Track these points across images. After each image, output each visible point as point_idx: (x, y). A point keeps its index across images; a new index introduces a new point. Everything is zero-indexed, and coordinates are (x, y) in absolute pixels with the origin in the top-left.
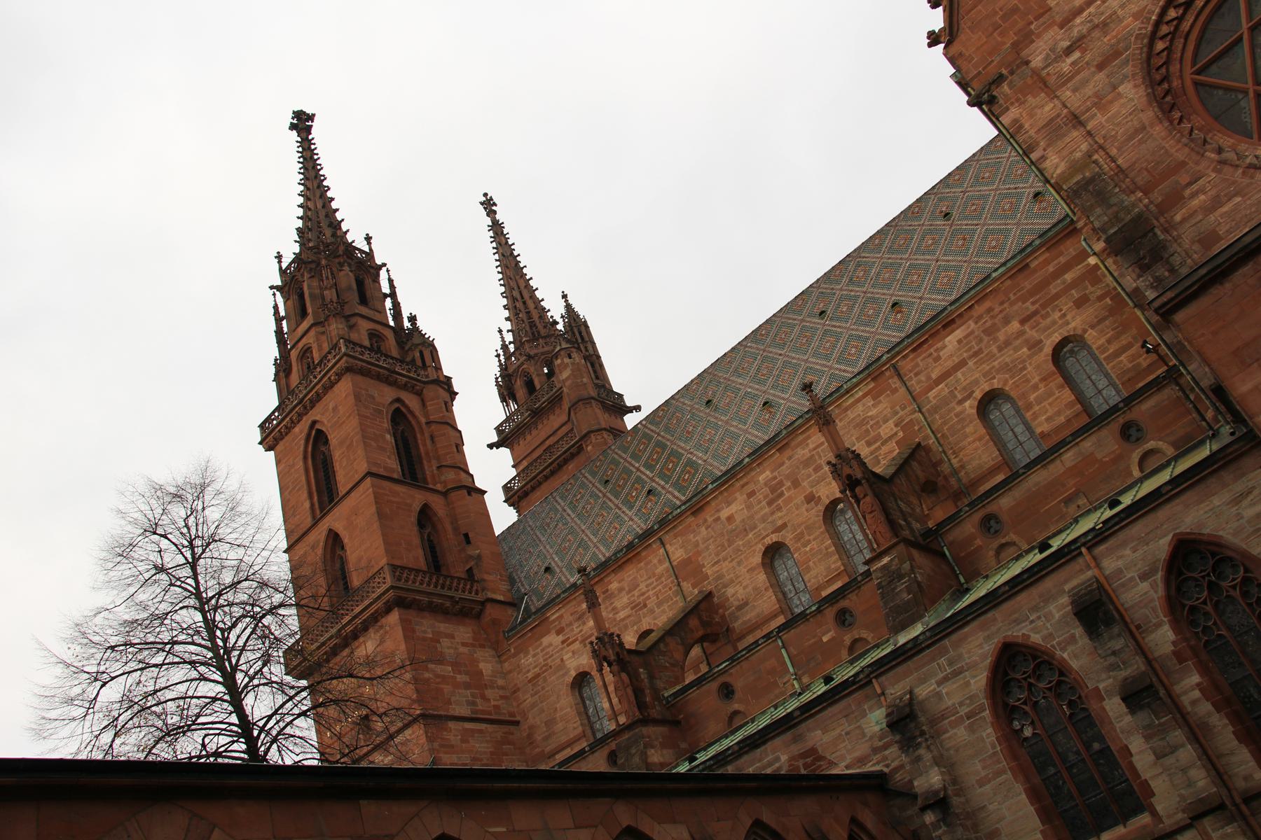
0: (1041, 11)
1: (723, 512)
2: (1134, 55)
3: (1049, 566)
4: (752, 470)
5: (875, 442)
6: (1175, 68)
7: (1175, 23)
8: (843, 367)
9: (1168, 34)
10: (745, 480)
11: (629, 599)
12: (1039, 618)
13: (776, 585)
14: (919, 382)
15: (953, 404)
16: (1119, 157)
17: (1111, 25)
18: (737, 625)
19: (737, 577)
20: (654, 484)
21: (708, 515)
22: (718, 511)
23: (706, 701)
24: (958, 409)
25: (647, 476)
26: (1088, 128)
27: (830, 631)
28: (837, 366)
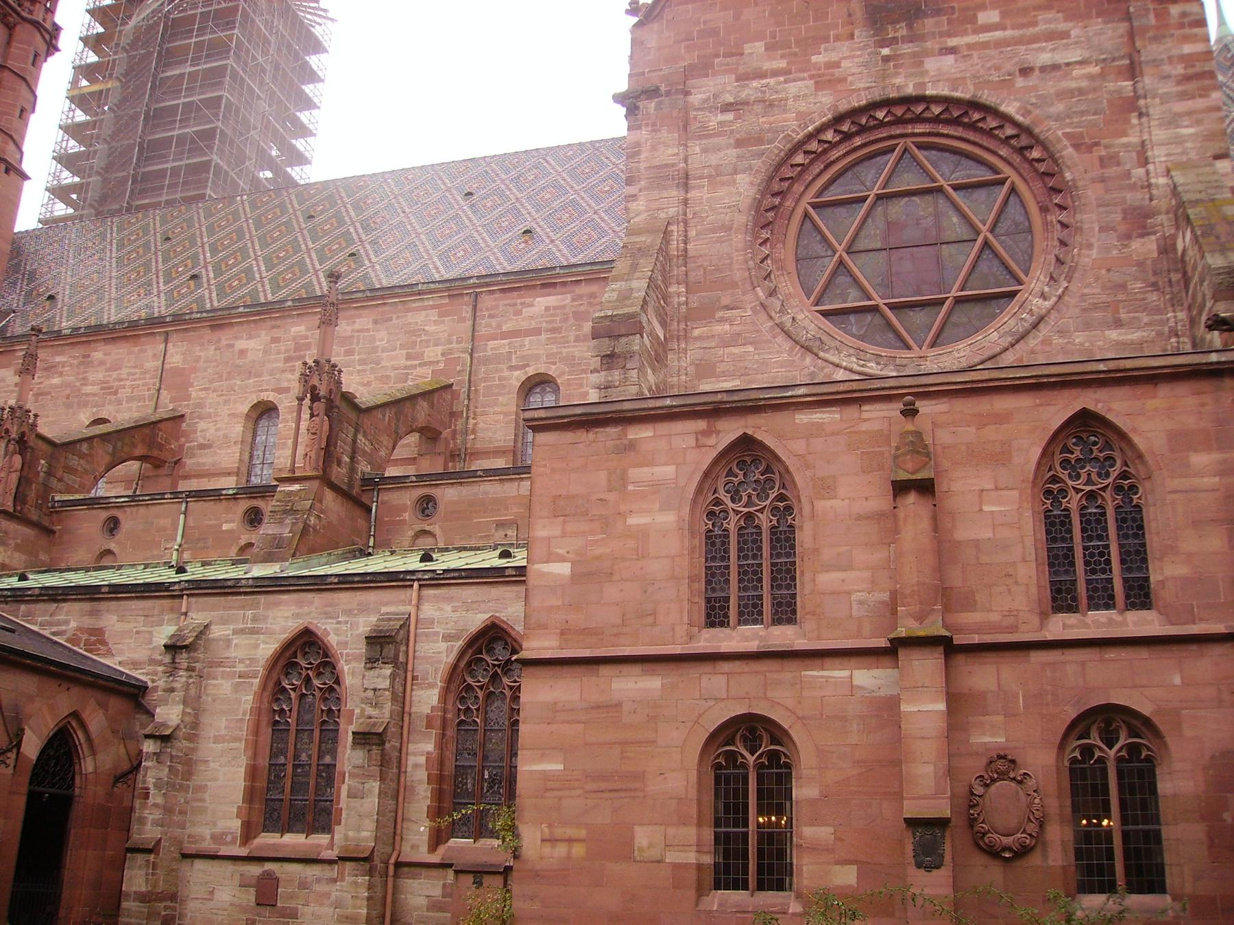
0: (734, 50)
1: (239, 342)
2: (772, 152)
3: (380, 582)
4: (290, 316)
5: (415, 359)
6: (798, 188)
7: (826, 146)
8: (439, 264)
9: (815, 152)
10: (278, 322)
11: (104, 376)
12: (346, 622)
13: (251, 444)
14: (489, 325)
16: (694, 241)
18: (189, 463)
19: (217, 415)
20: (204, 272)
21: (225, 337)
22: (236, 338)
23: (89, 524)
24: (506, 373)
25: (205, 258)
27: (232, 521)
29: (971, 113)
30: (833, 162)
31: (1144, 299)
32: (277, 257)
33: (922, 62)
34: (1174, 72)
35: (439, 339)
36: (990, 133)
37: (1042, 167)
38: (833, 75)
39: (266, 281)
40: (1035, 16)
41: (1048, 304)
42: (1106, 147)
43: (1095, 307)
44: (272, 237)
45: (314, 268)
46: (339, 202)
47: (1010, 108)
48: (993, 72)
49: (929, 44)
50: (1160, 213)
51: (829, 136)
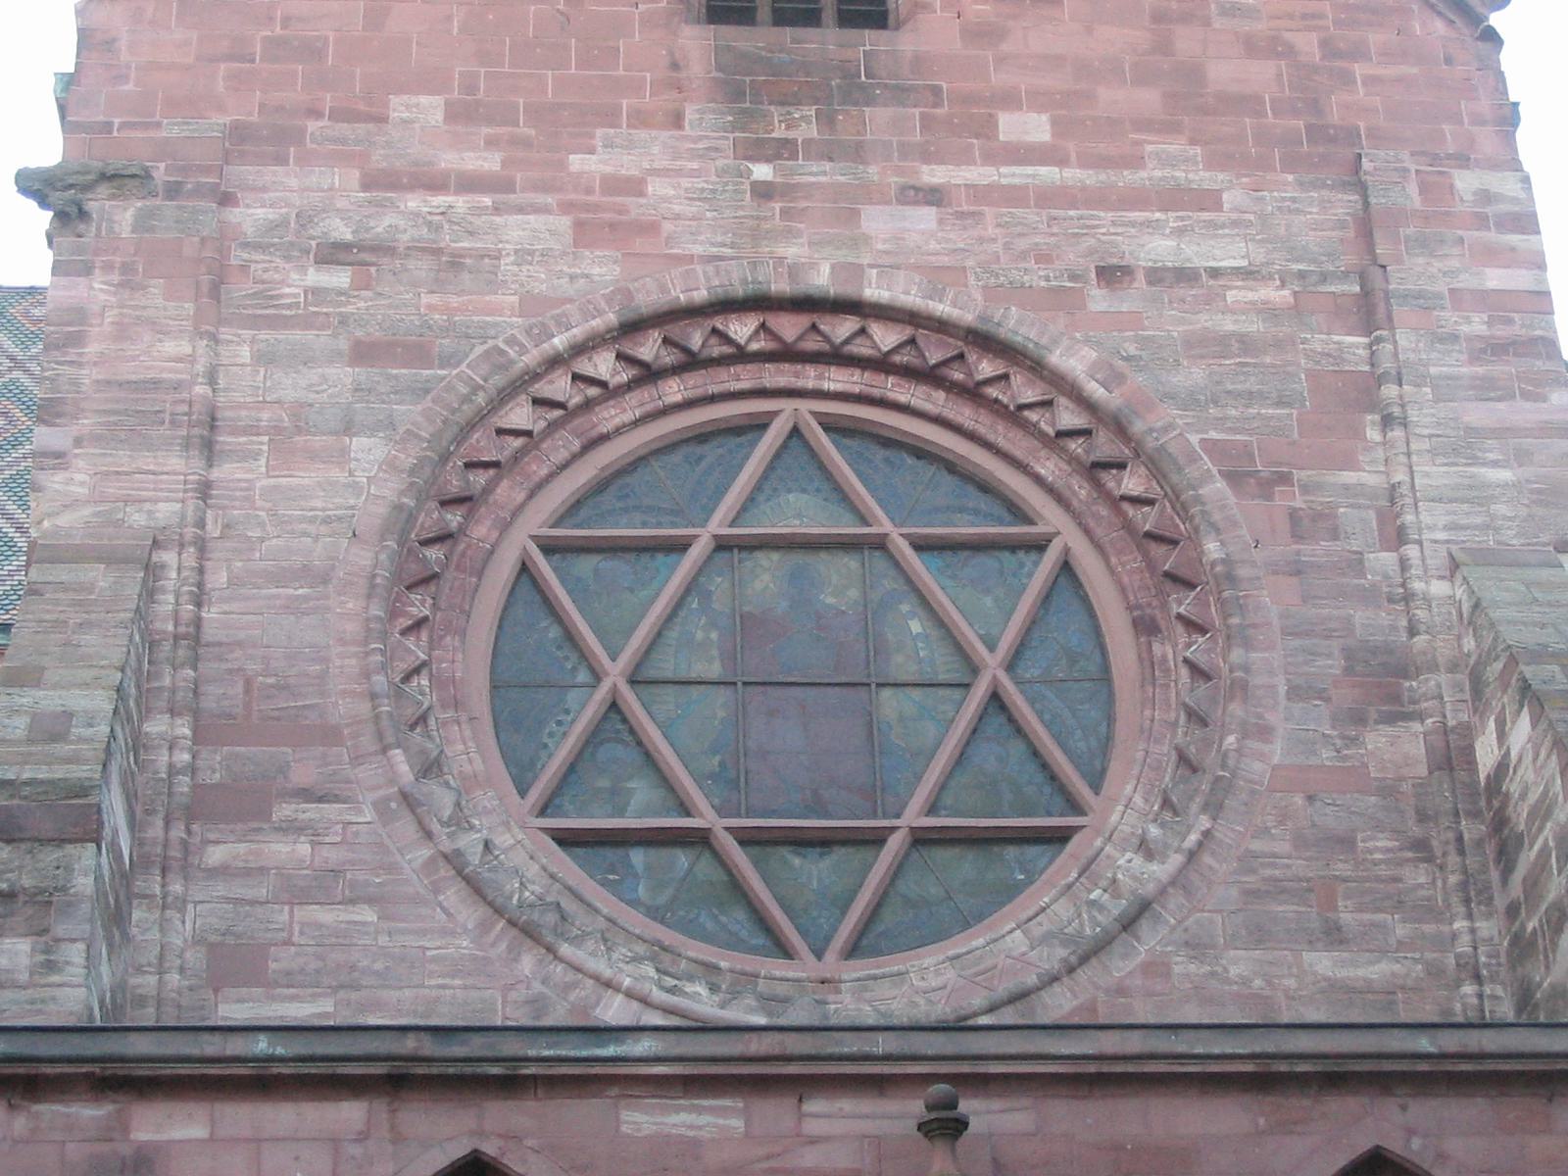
0: (362, 107)
2: (450, 388)
7: (593, 391)
17: (466, 276)
26: (215, 474)
29: (972, 357)
30: (604, 438)
31: (1396, 880)
33: (855, 213)
34: (1465, 329)
36: (1014, 416)
37: (1146, 519)
38: (622, 210)
40: (1137, 143)
41: (1160, 870)
42: (1305, 489)
43: (1277, 889)
47: (1074, 361)
48: (1031, 264)
49: (873, 171)
50: (1433, 667)
51: (603, 365)
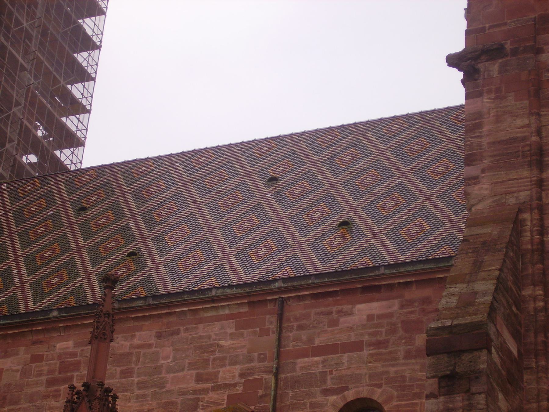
4: (58, 330)
5: (207, 381)
8: (237, 265)
10: (41, 337)
15: (317, 390)
24: (320, 399)
28: (233, 259)
32: (42, 258)
35: (237, 356)
39: (27, 286)
44: (35, 233)
45: (86, 271)
46: (117, 191)
